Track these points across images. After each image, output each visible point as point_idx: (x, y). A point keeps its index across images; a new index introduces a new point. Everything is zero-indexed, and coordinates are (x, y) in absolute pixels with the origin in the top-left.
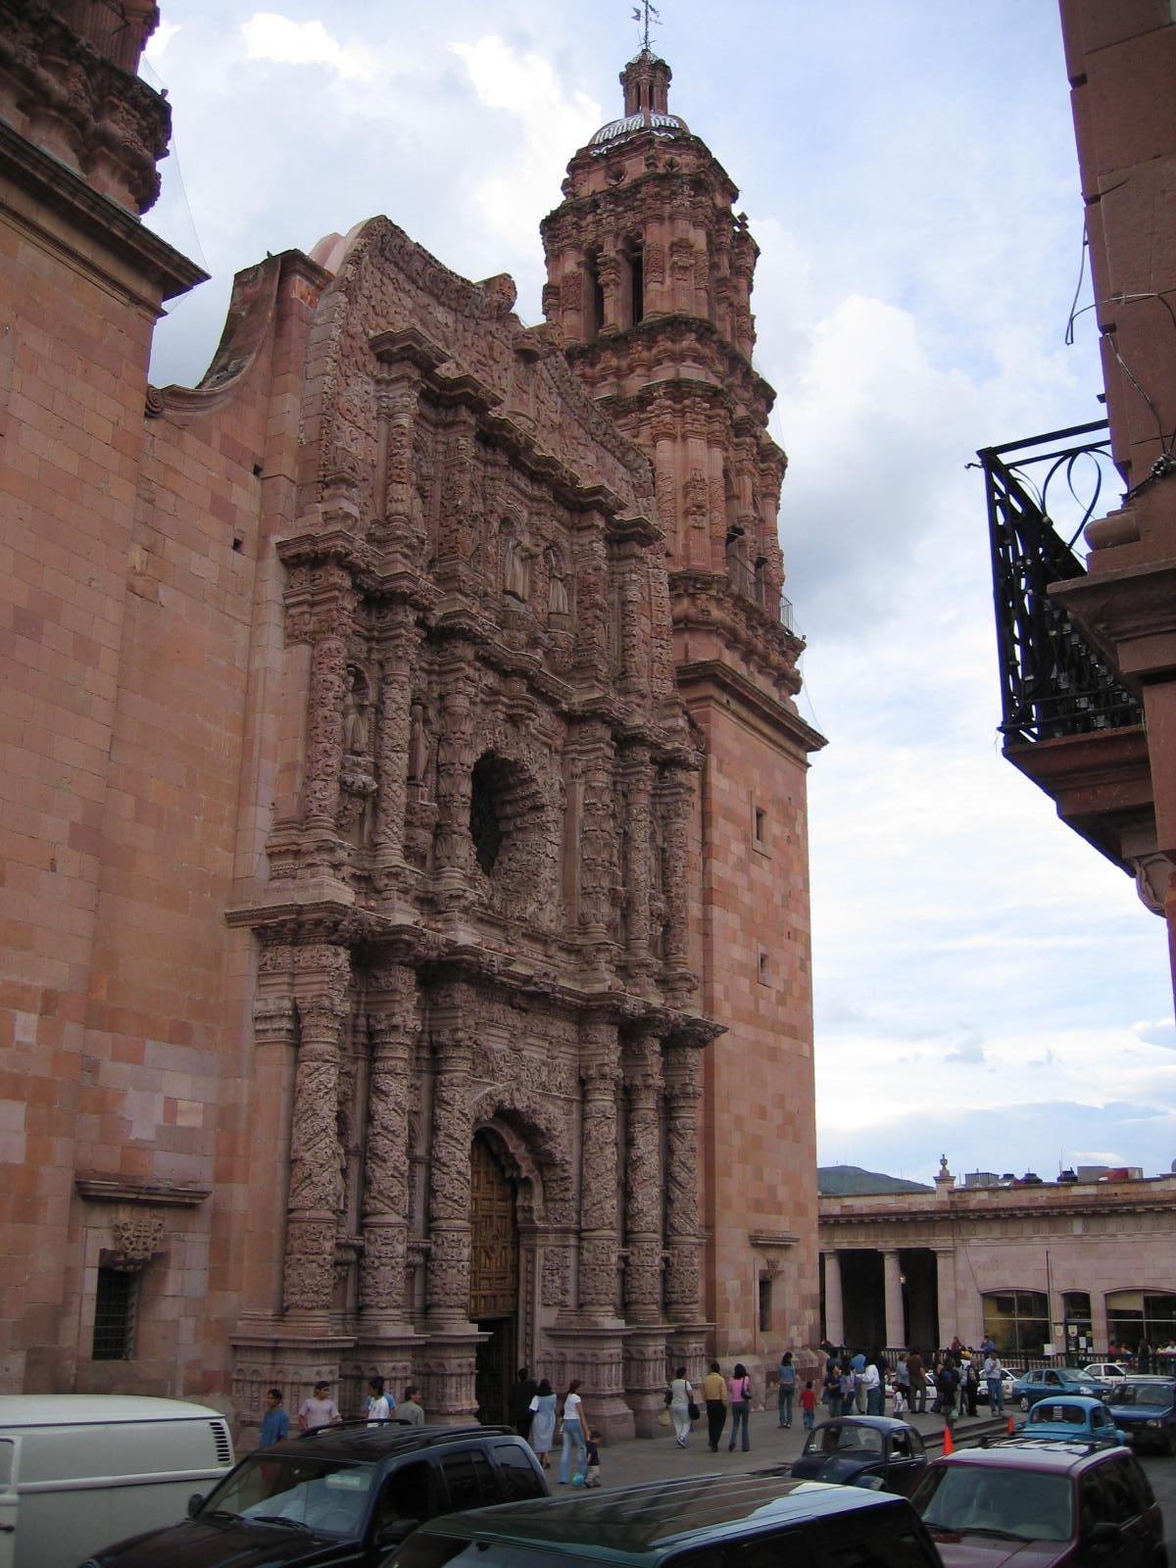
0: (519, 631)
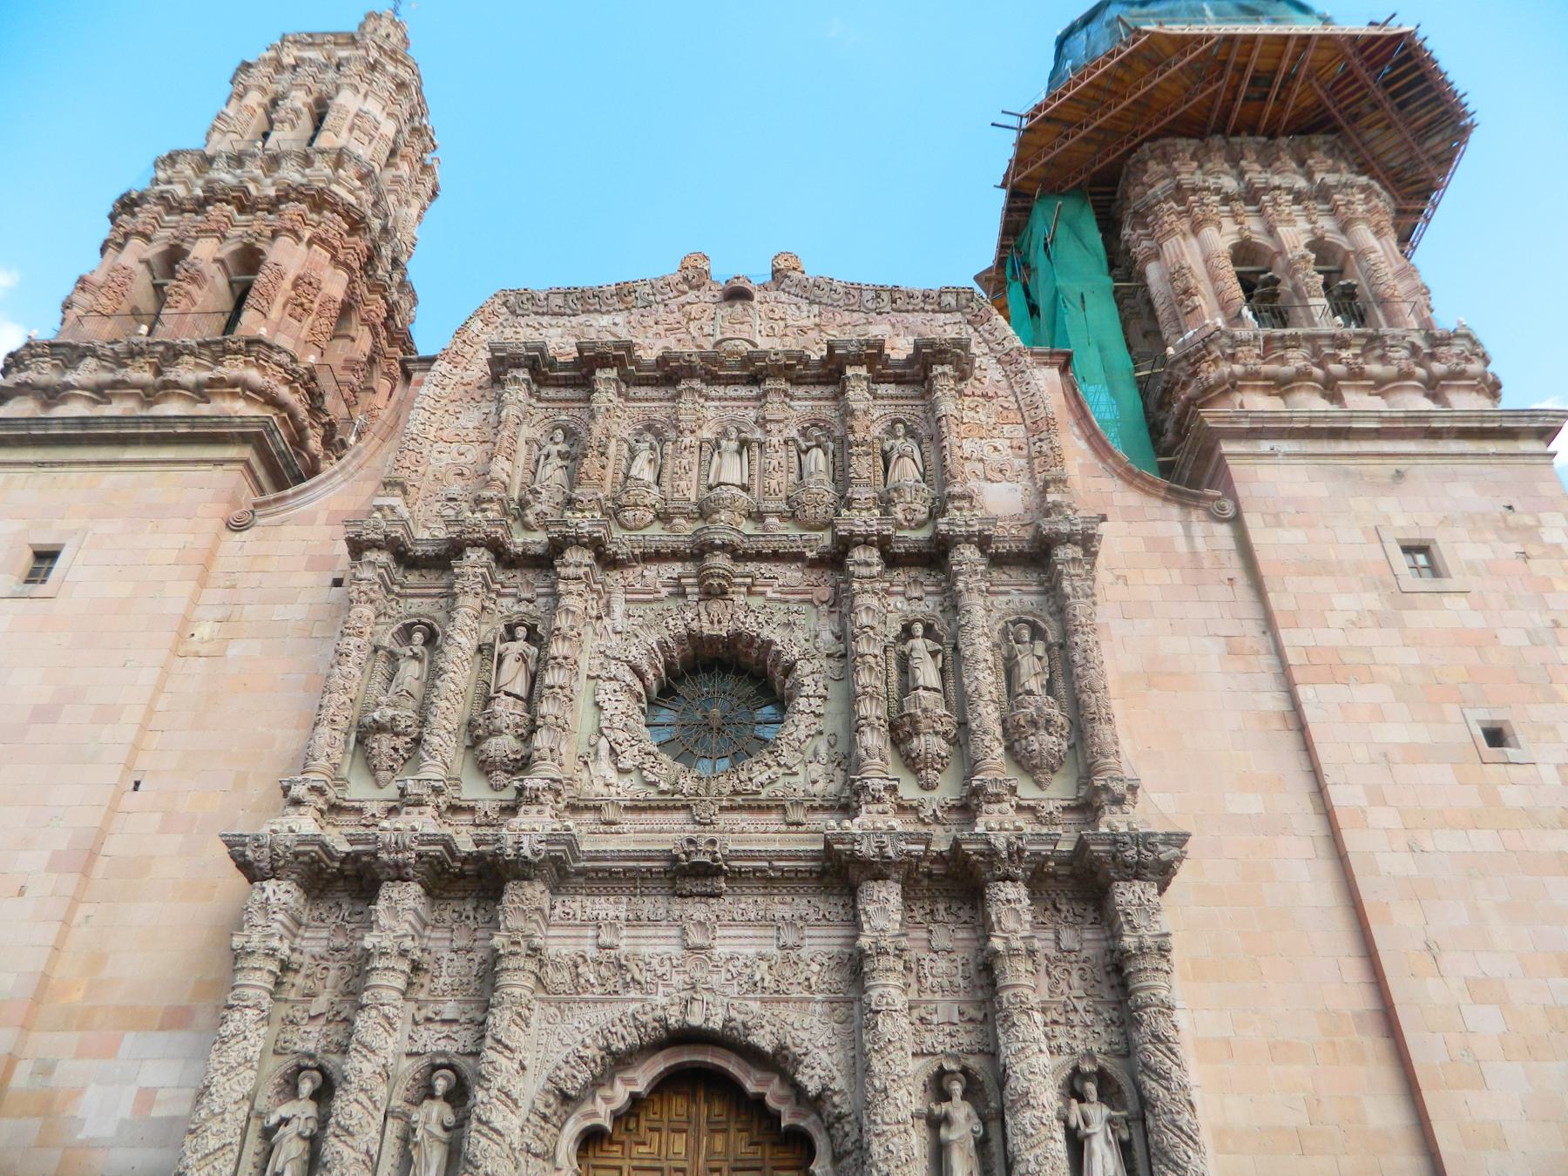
0: (718, 512)
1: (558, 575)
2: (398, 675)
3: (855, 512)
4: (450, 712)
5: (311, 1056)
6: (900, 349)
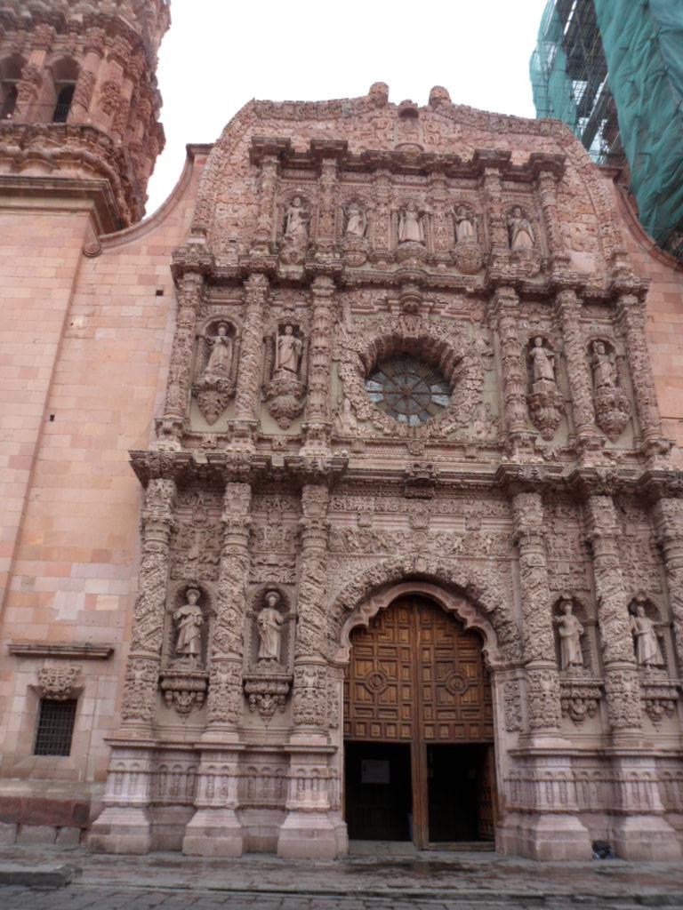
1: (313, 295)
2: (212, 355)
3: (501, 265)
4: (248, 381)
5: (195, 582)
6: (519, 158)
